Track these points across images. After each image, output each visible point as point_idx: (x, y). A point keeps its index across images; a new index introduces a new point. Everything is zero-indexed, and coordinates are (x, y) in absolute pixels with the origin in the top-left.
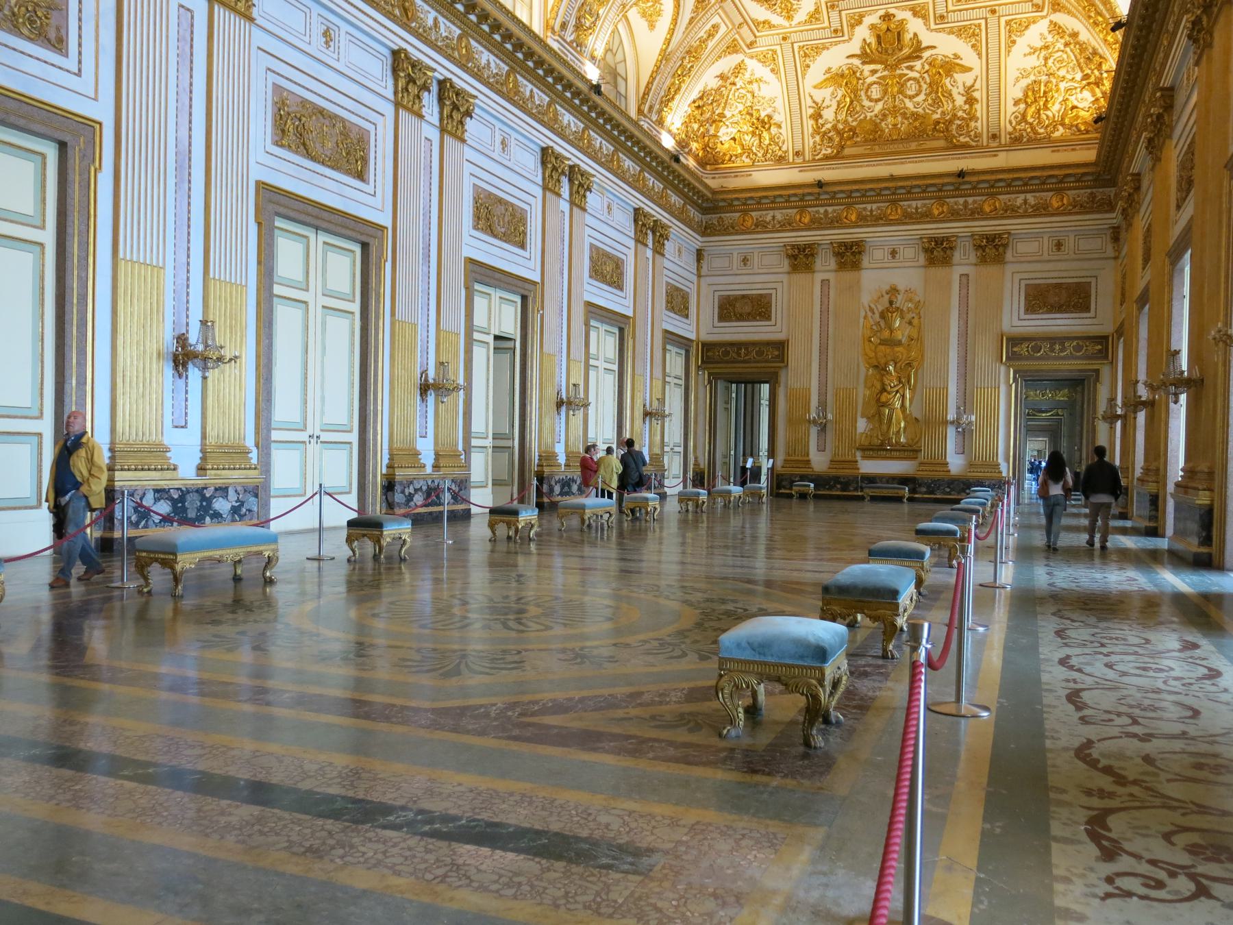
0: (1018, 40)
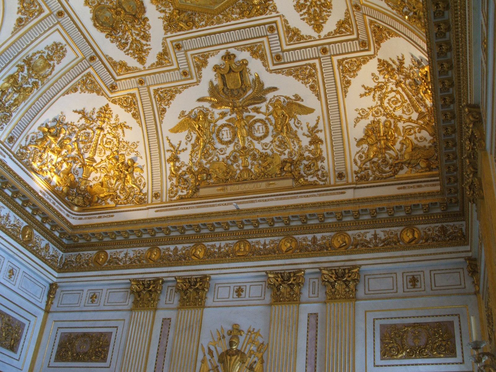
0: (352, 80)
